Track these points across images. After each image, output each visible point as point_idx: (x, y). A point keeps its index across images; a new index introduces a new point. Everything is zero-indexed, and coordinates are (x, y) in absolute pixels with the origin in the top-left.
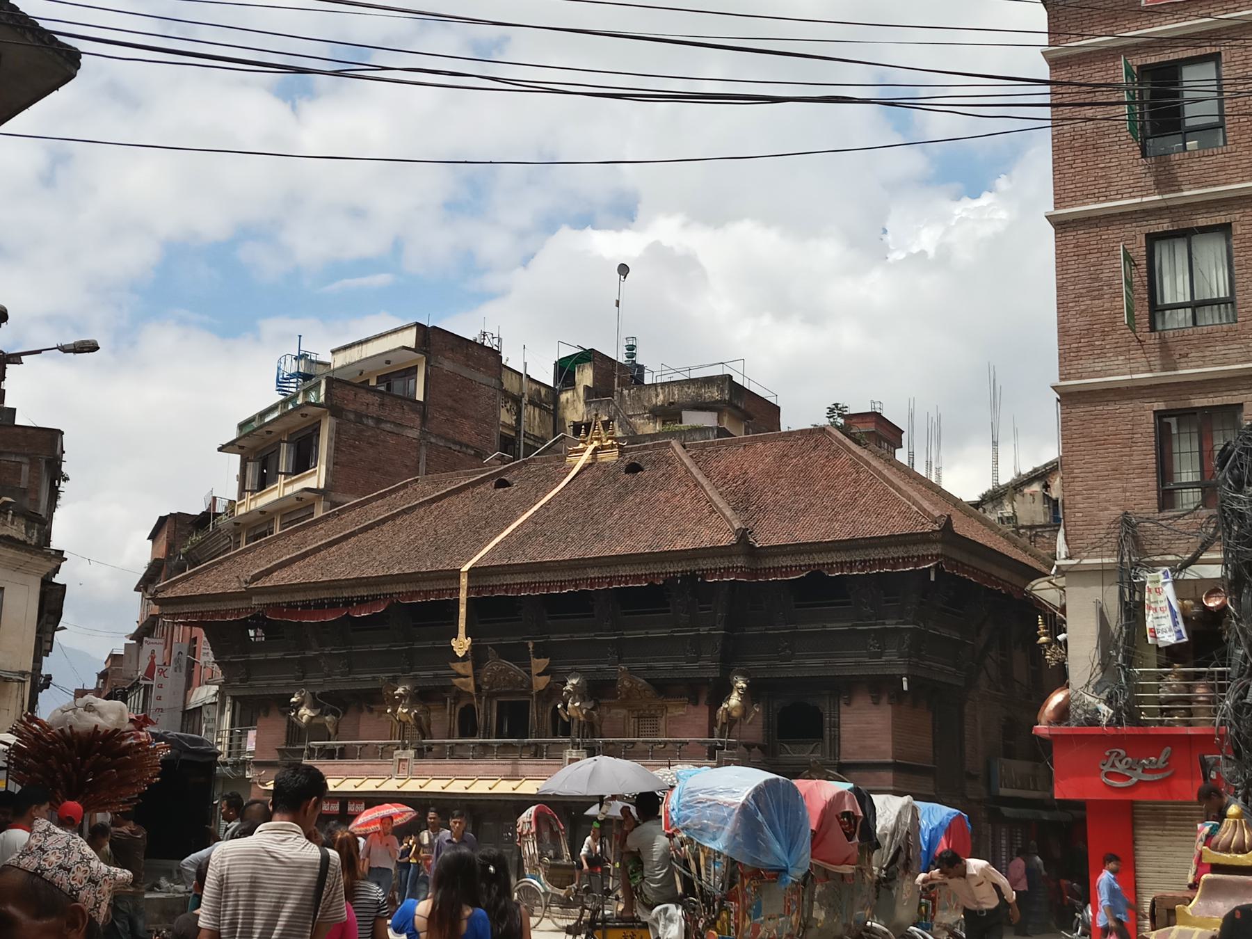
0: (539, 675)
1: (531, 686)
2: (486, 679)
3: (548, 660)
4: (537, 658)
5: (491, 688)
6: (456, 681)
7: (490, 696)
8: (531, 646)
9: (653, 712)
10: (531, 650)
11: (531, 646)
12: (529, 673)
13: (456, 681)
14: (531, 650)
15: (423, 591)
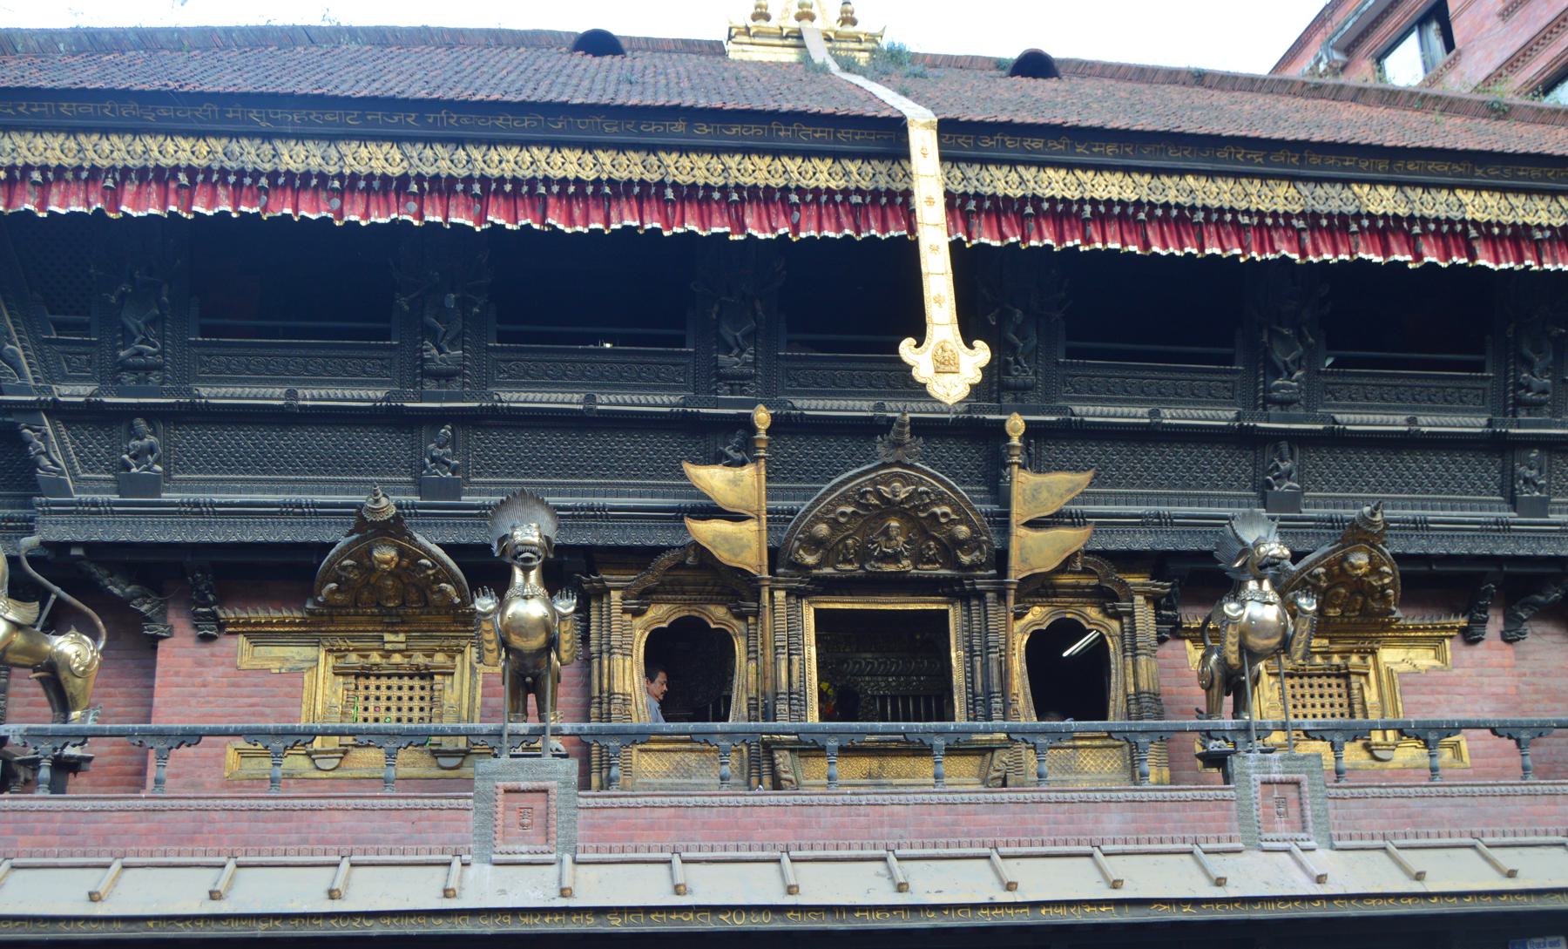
0: (1033, 524)
1: (1000, 559)
2: (822, 529)
3: (1083, 478)
4: (1034, 463)
5: (818, 566)
6: (706, 531)
7: (796, 594)
8: (1016, 424)
9: (1336, 659)
10: (1015, 441)
11: (1016, 424)
12: (1002, 523)
13: (706, 531)
14: (1015, 441)
15: (675, 185)
